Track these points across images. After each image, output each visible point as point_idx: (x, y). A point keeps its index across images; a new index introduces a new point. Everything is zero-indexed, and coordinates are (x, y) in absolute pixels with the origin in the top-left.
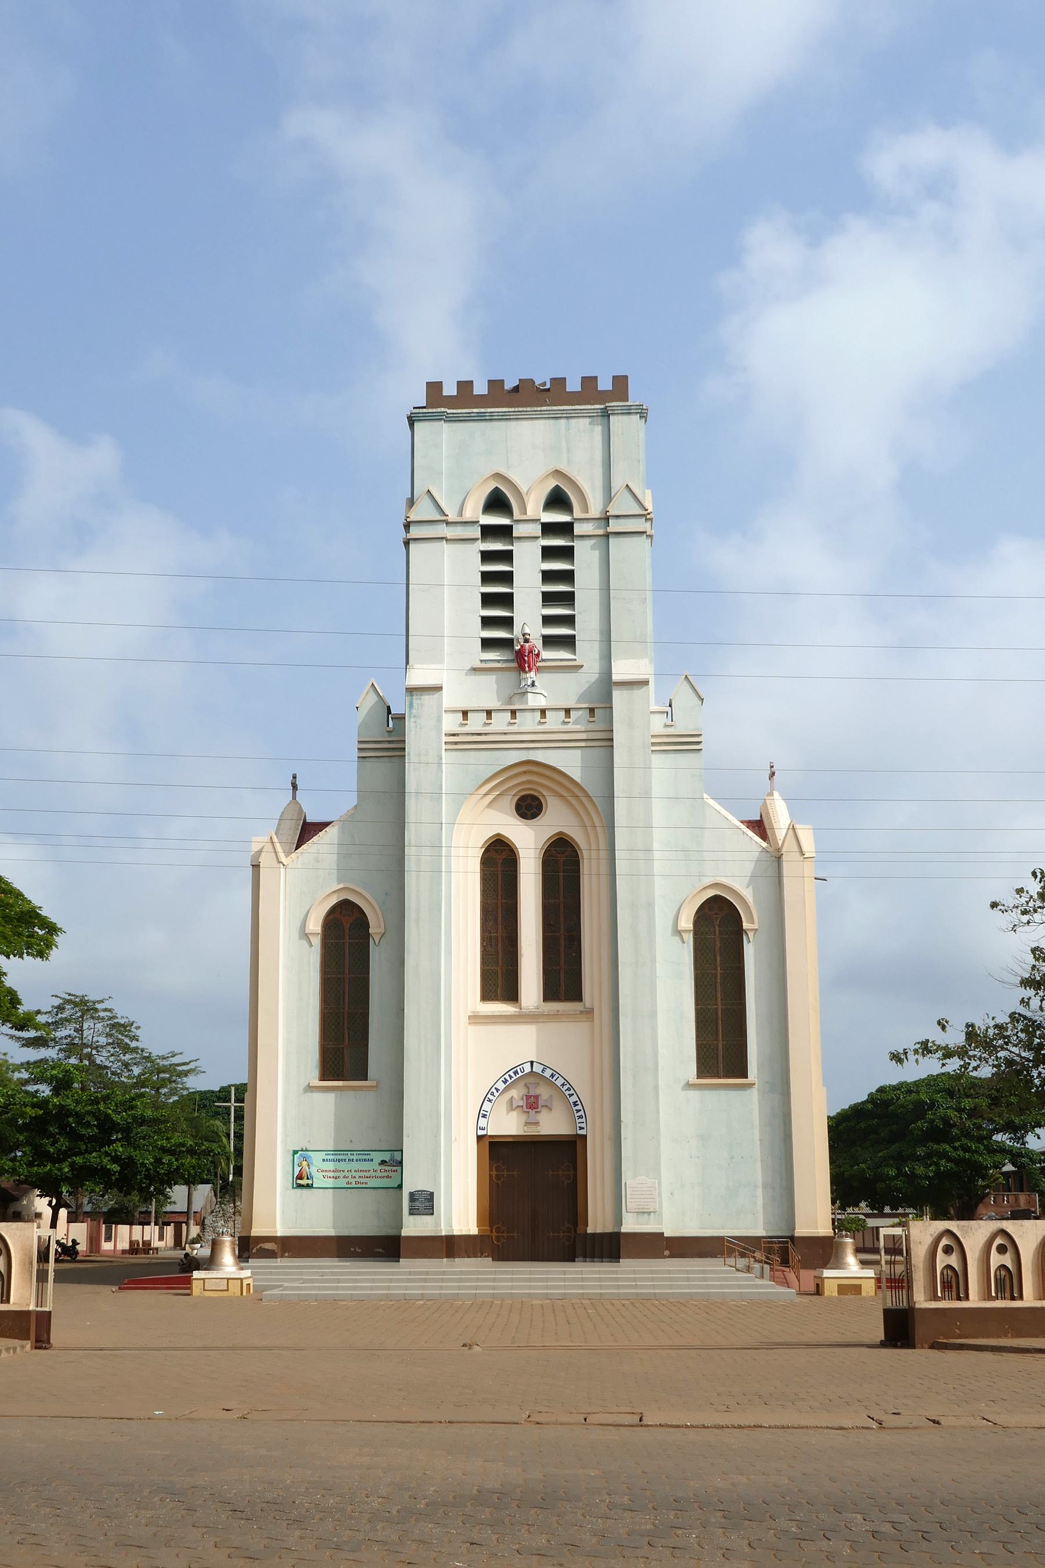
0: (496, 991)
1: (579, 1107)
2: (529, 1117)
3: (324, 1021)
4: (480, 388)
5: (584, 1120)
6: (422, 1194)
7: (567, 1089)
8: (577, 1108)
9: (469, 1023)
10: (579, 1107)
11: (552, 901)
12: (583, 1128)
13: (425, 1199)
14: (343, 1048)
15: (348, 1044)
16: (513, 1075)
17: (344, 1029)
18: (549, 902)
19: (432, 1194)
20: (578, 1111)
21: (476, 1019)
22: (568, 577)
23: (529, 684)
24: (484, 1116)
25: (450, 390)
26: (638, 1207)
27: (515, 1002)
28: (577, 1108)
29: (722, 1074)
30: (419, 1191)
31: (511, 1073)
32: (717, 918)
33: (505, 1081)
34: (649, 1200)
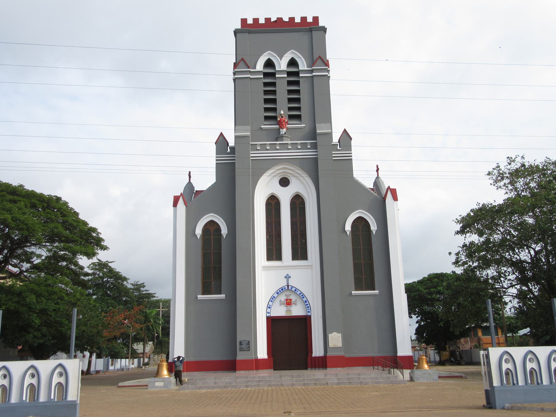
0: (273, 257)
1: (307, 303)
2: (287, 308)
3: (203, 270)
4: (262, 21)
5: (309, 308)
7: (302, 296)
8: (307, 303)
9: (262, 270)
10: (307, 303)
11: (294, 220)
12: (309, 312)
13: (246, 344)
14: (211, 281)
15: (213, 279)
16: (281, 290)
17: (211, 274)
18: (293, 220)
19: (249, 342)
20: (307, 305)
21: (265, 268)
22: (298, 92)
23: (284, 133)
24: (269, 308)
25: (250, 21)
26: (334, 345)
27: (280, 261)
28: (307, 303)
29: (364, 289)
30: (243, 341)
32: (360, 226)
33: (277, 293)
34: (338, 342)
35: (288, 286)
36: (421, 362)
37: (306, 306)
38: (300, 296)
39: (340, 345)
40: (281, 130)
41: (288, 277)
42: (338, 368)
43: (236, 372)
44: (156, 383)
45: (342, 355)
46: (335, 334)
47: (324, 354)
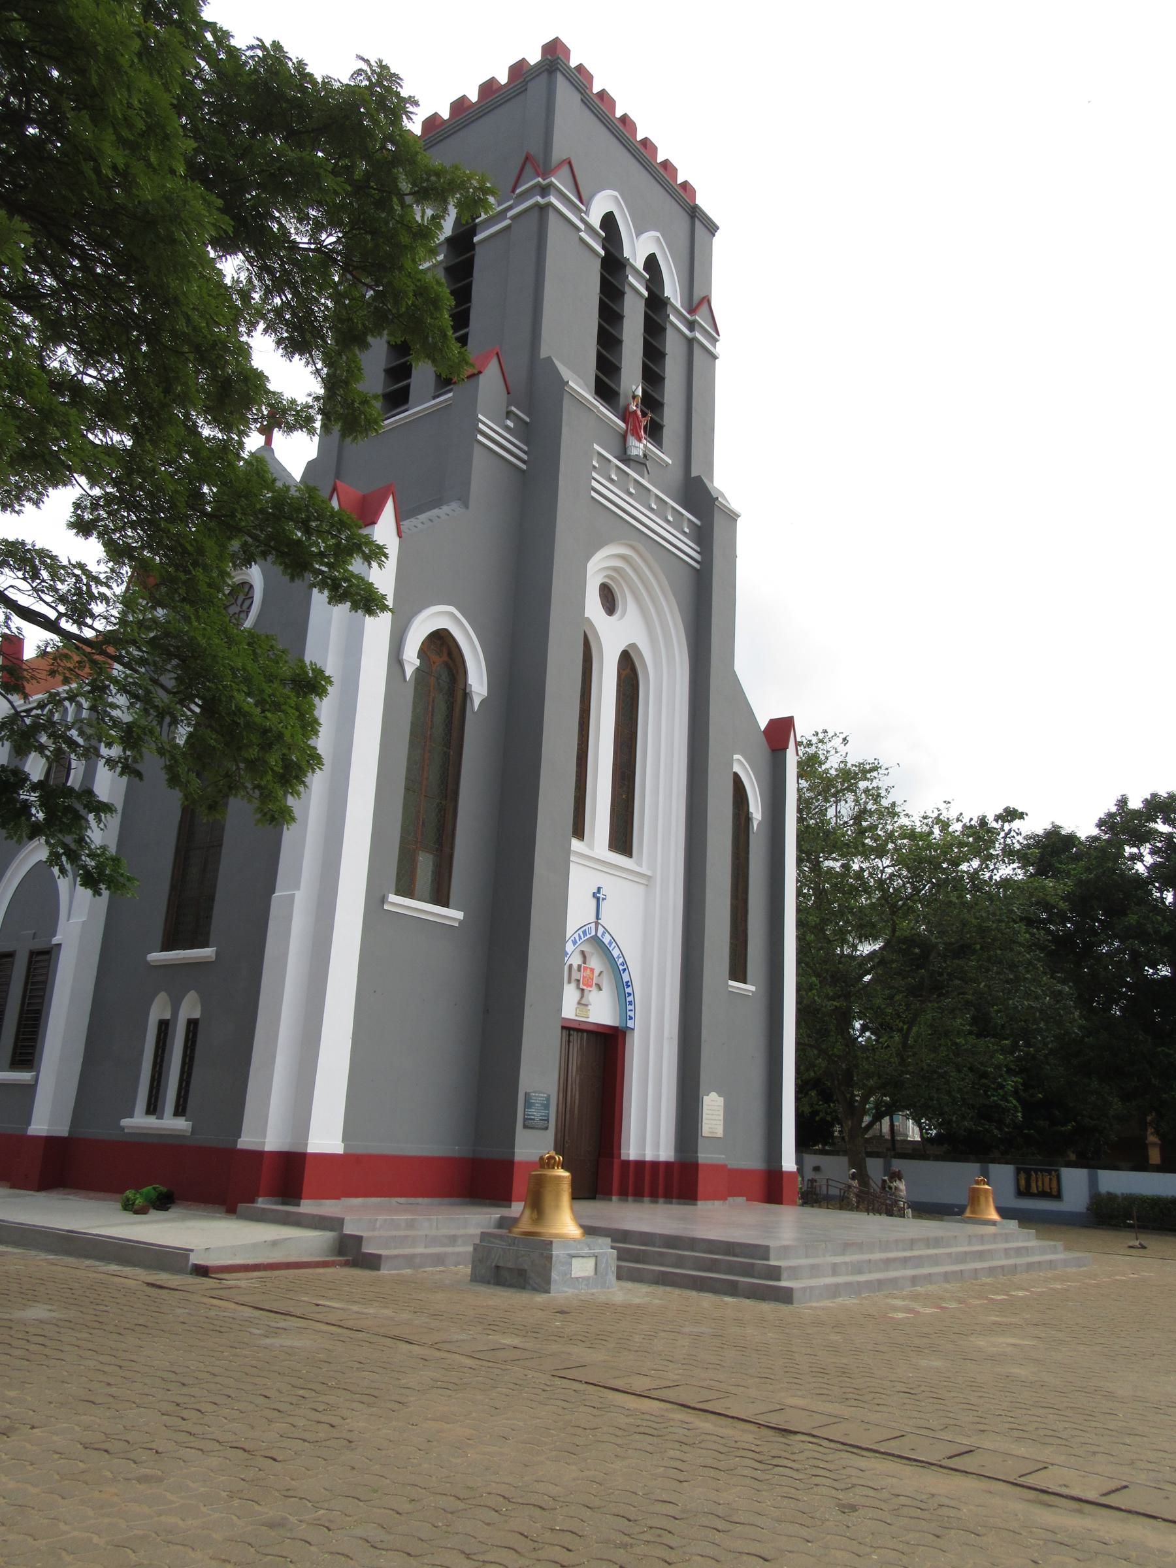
1: (629, 990)
6: (538, 1096)
10: (629, 990)
19: (548, 1099)
20: (629, 994)
31: (580, 932)
35: (597, 924)
36: (982, 1199)
37: (628, 999)
38: (619, 963)
39: (719, 1131)
40: (632, 441)
41: (603, 899)
42: (716, 1203)
43: (510, 1207)
44: (574, 1261)
45: (722, 1162)
46: (713, 1095)
47: (675, 1156)
